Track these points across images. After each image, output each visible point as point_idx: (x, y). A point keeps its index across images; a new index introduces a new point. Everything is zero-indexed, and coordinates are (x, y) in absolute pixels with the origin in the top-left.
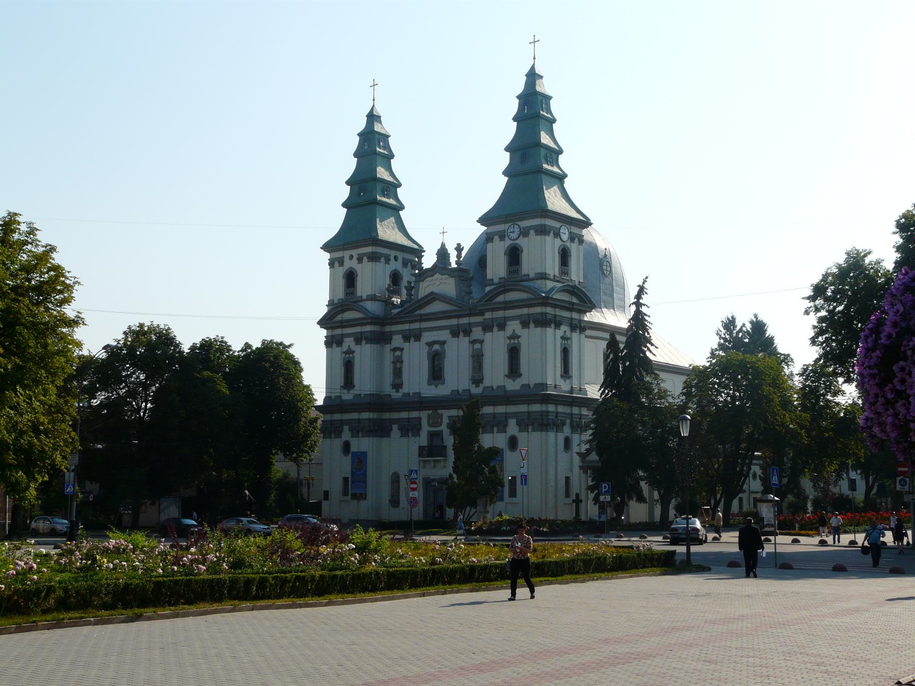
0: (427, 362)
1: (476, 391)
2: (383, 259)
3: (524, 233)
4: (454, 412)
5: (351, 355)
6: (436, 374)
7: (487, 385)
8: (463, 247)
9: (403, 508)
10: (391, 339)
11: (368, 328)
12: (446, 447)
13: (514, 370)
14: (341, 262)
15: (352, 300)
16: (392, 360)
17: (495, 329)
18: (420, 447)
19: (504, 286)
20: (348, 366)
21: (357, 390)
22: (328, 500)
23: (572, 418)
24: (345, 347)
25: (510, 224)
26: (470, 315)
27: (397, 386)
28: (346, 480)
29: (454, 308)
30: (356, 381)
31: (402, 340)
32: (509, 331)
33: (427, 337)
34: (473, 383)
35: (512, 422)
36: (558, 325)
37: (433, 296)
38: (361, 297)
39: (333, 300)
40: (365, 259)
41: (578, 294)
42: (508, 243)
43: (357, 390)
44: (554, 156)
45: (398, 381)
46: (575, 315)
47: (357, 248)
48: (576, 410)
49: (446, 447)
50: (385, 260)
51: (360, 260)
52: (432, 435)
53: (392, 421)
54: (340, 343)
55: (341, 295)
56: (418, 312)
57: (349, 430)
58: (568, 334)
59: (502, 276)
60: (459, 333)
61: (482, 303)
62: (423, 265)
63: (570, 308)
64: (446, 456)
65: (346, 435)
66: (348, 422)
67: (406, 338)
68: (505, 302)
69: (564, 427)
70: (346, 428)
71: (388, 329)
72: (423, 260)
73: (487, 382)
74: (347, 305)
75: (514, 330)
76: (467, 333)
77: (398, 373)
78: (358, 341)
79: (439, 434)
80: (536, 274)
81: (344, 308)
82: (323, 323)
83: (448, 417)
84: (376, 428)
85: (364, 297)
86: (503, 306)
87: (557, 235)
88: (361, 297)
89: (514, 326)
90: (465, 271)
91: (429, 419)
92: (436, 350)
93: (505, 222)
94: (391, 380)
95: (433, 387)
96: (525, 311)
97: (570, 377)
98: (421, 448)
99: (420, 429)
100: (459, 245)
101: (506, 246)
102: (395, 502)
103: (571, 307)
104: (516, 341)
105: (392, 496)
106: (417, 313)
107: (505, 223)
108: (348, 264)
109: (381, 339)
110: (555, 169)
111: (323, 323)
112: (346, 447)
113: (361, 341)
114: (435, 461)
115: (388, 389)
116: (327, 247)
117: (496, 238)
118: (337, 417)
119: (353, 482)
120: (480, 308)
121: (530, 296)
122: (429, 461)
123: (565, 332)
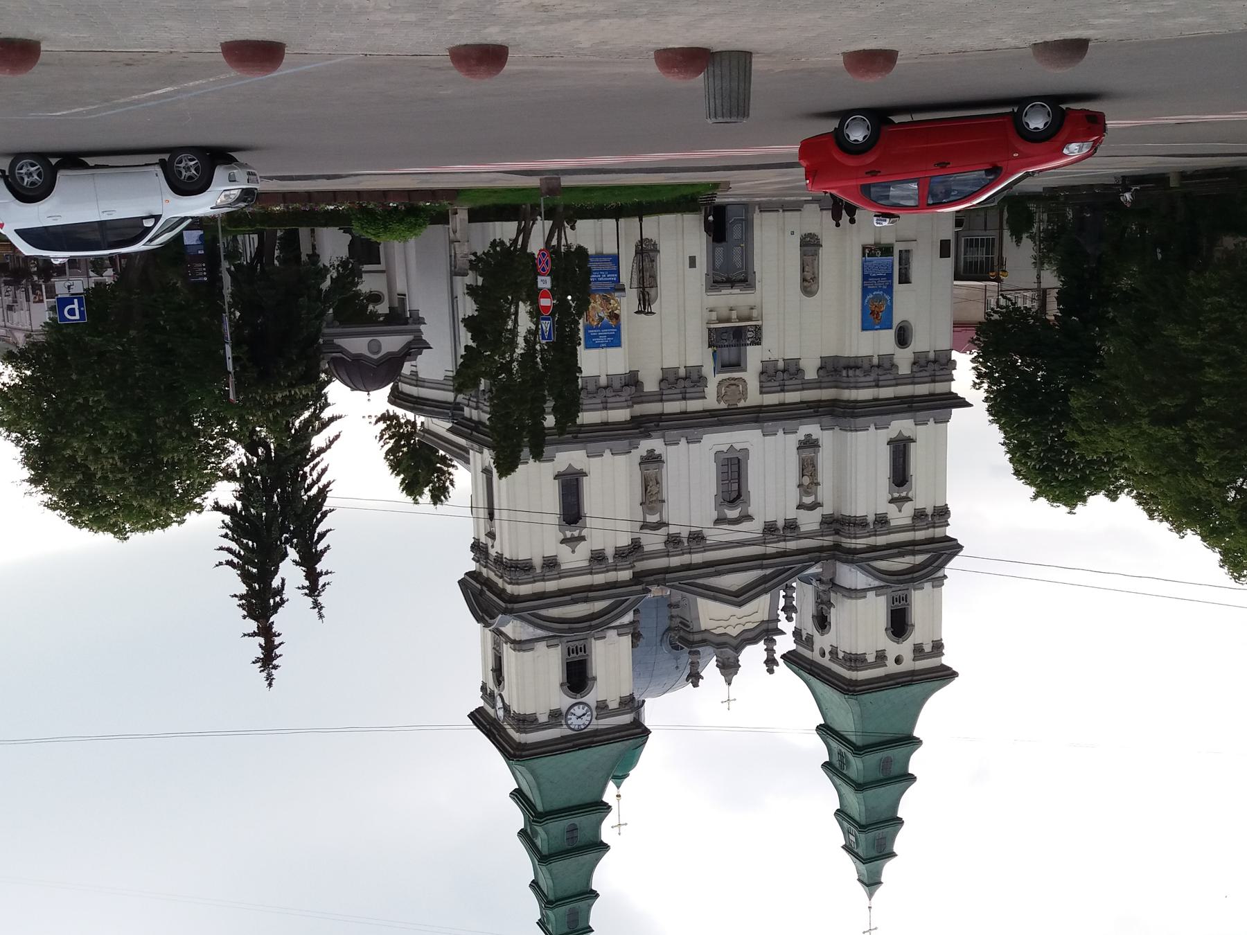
0: (750, 488)
1: (654, 444)
2: (841, 655)
3: (556, 716)
4: (694, 405)
5: (896, 495)
7: (623, 457)
8: (687, 680)
9: (793, 233)
10: (822, 523)
11: (861, 543)
12: (710, 346)
13: (571, 486)
14: (918, 651)
15: (894, 589)
17: (610, 552)
19: (596, 624)
20: (900, 476)
21: (884, 435)
22: (941, 241)
24: (908, 508)
25: (584, 731)
26: (668, 570)
27: (809, 444)
28: (905, 279)
29: (700, 581)
31: (799, 522)
32: (583, 550)
33: (752, 529)
34: (660, 455)
36: (499, 560)
37: (742, 598)
38: (877, 595)
39: (933, 587)
40: (871, 658)
42: (591, 698)
43: (884, 435)
45: (807, 453)
47: (886, 676)
49: (710, 346)
50: (837, 654)
51: (881, 657)
52: (738, 365)
53: (817, 384)
54: (919, 515)
55: (919, 599)
56: (769, 571)
57: (897, 367)
59: (599, 643)
60: (689, 538)
62: (765, 647)
64: (709, 329)
65: (904, 360)
66: (899, 381)
67: (791, 526)
68: (586, 600)
70: (904, 369)
71: (828, 541)
72: (764, 656)
75: (573, 552)
77: (808, 469)
78: (882, 520)
79: (723, 366)
80: (532, 649)
81: (910, 576)
82: (951, 548)
83: (705, 398)
84: (844, 373)
85: (871, 594)
86: (591, 594)
87: (506, 708)
88: (877, 595)
91: (744, 394)
93: (596, 732)
94: (820, 455)
95: (738, 447)
96: (551, 586)
98: (757, 341)
99: (762, 373)
100: (695, 685)
102: (810, 244)
104: (569, 534)
105: (816, 254)
106: (769, 571)
107: (597, 730)
108: (905, 648)
109: (836, 523)
111: (951, 548)
112: (903, 337)
113: (876, 520)
114: (728, 320)
115: (827, 438)
116: (947, 675)
117: (613, 705)
118: (922, 389)
119: (890, 276)
120: (639, 587)
121: (543, 612)
122: (740, 319)
123: (493, 546)
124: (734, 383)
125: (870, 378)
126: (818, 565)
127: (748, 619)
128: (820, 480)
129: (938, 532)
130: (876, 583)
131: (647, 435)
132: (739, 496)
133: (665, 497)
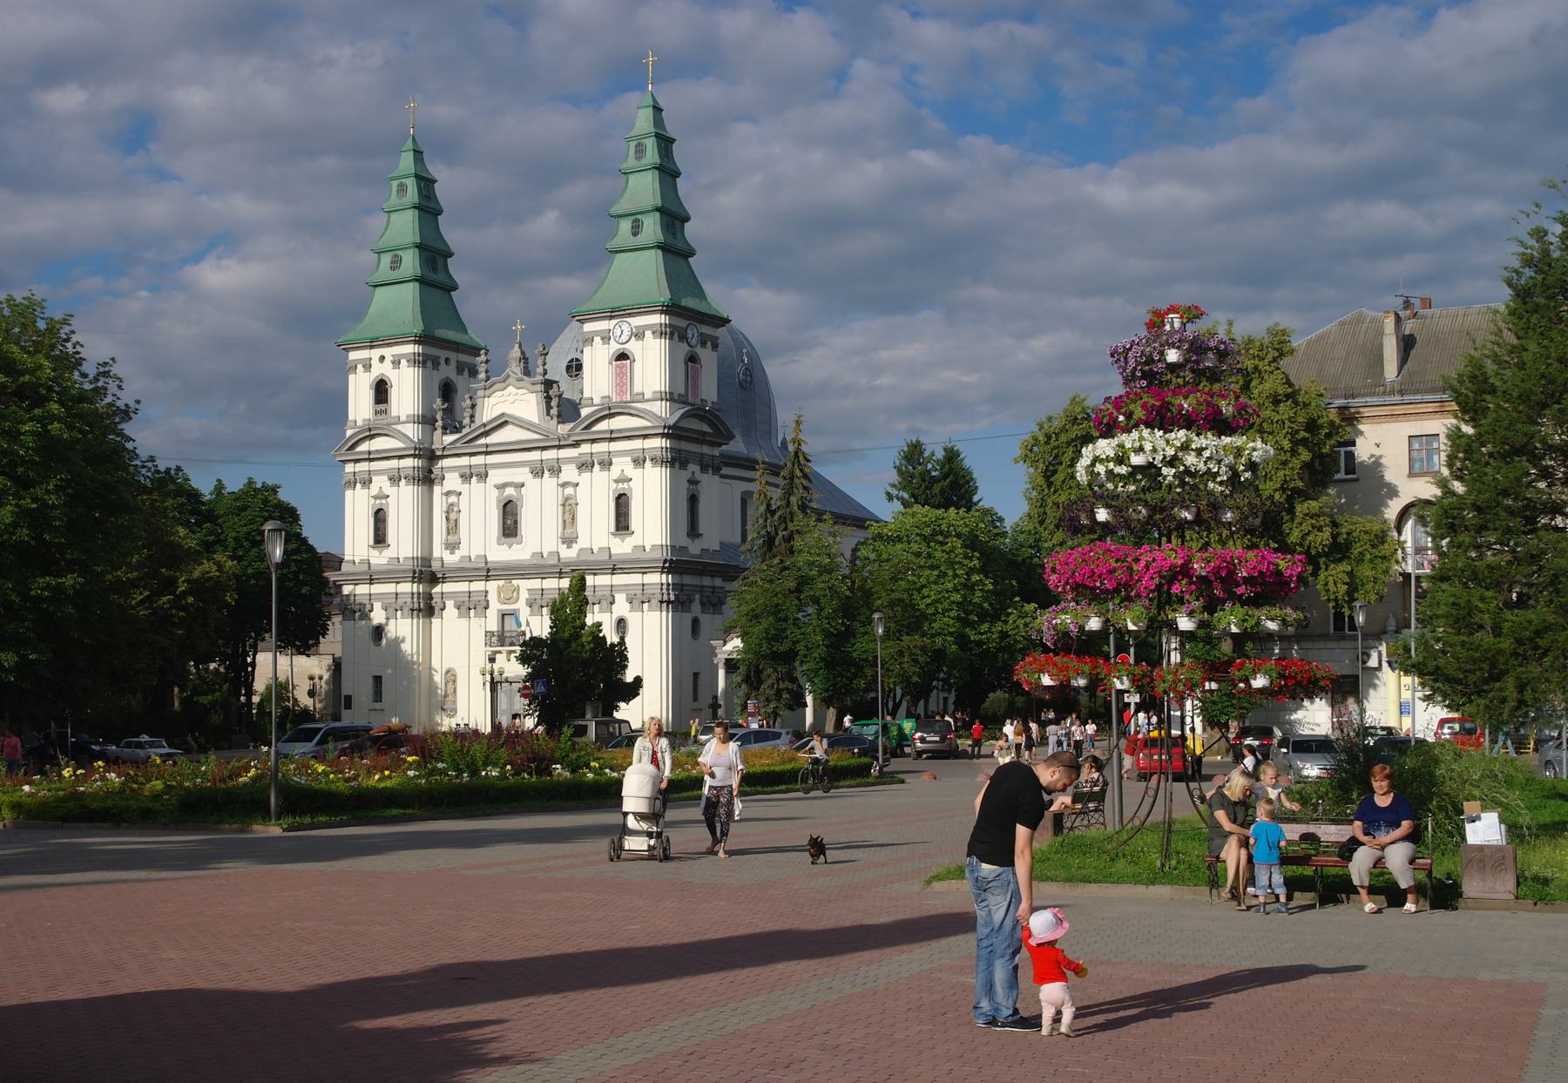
1: (569, 554)
2: (429, 364)
3: (639, 334)
4: (536, 584)
5: (384, 501)
6: (510, 529)
10: (443, 479)
14: (368, 366)
15: (385, 422)
16: (445, 509)
17: (597, 467)
18: (486, 632)
23: (702, 591)
26: (560, 447)
27: (452, 547)
30: (391, 537)
32: (615, 471)
33: (496, 477)
34: (563, 543)
35: (621, 598)
36: (684, 465)
40: (404, 362)
41: (709, 420)
42: (614, 347)
44: (678, 224)
46: (706, 449)
48: (707, 581)
51: (396, 363)
52: (503, 616)
56: (482, 441)
58: (699, 476)
61: (578, 430)
63: (700, 439)
66: (381, 596)
67: (466, 477)
69: (693, 604)
73: (583, 542)
74: (378, 428)
76: (556, 470)
77: (453, 527)
78: (395, 480)
80: (654, 393)
84: (422, 605)
85: (403, 418)
87: (683, 337)
89: (622, 465)
90: (548, 384)
91: (500, 590)
92: (510, 495)
93: (611, 318)
97: (699, 535)
99: (486, 608)
101: (611, 353)
103: (701, 437)
108: (378, 370)
110: (680, 245)
117: (597, 340)
118: (362, 589)
124: (508, 600)
125: (404, 600)
126: (445, 443)
127: (501, 400)
128: (444, 515)
129: (349, 468)
130: (399, 427)
131: (567, 564)
132: (505, 506)
133: (560, 508)
